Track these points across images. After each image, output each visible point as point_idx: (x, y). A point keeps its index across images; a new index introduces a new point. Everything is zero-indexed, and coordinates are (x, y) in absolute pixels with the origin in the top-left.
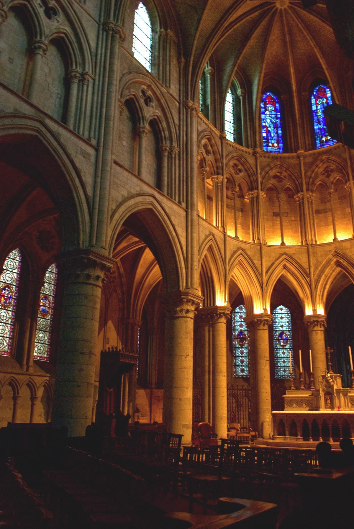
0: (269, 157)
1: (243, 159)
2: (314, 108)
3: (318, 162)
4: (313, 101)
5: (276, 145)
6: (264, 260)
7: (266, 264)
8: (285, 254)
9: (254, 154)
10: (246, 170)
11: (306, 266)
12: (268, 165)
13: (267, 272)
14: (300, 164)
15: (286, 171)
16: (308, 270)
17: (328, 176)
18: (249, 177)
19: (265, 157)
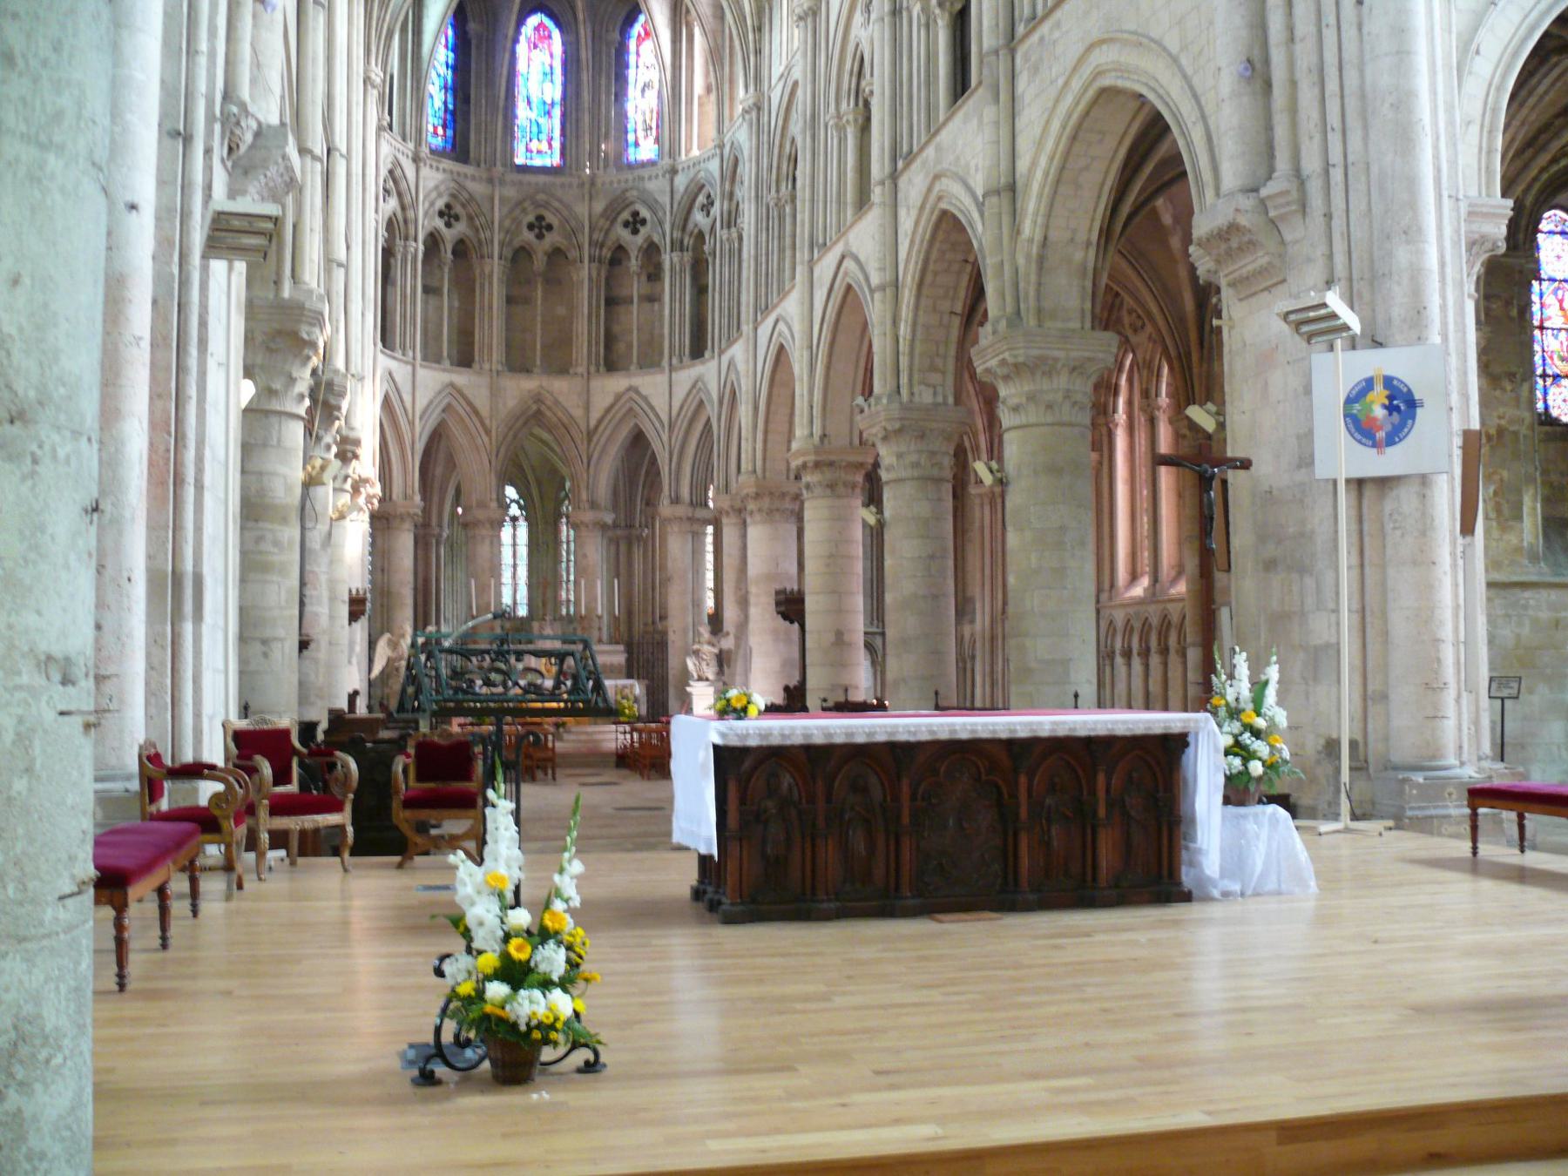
0: (438, 169)
1: (399, 170)
2: (521, 66)
3: (526, 204)
4: (522, 49)
5: (440, 131)
6: (418, 394)
7: (421, 404)
8: (452, 385)
9: (416, 159)
10: (400, 195)
11: (484, 412)
12: (436, 187)
13: (421, 418)
14: (492, 199)
15: (463, 206)
16: (487, 422)
17: (540, 237)
18: (403, 208)
19: (431, 166)
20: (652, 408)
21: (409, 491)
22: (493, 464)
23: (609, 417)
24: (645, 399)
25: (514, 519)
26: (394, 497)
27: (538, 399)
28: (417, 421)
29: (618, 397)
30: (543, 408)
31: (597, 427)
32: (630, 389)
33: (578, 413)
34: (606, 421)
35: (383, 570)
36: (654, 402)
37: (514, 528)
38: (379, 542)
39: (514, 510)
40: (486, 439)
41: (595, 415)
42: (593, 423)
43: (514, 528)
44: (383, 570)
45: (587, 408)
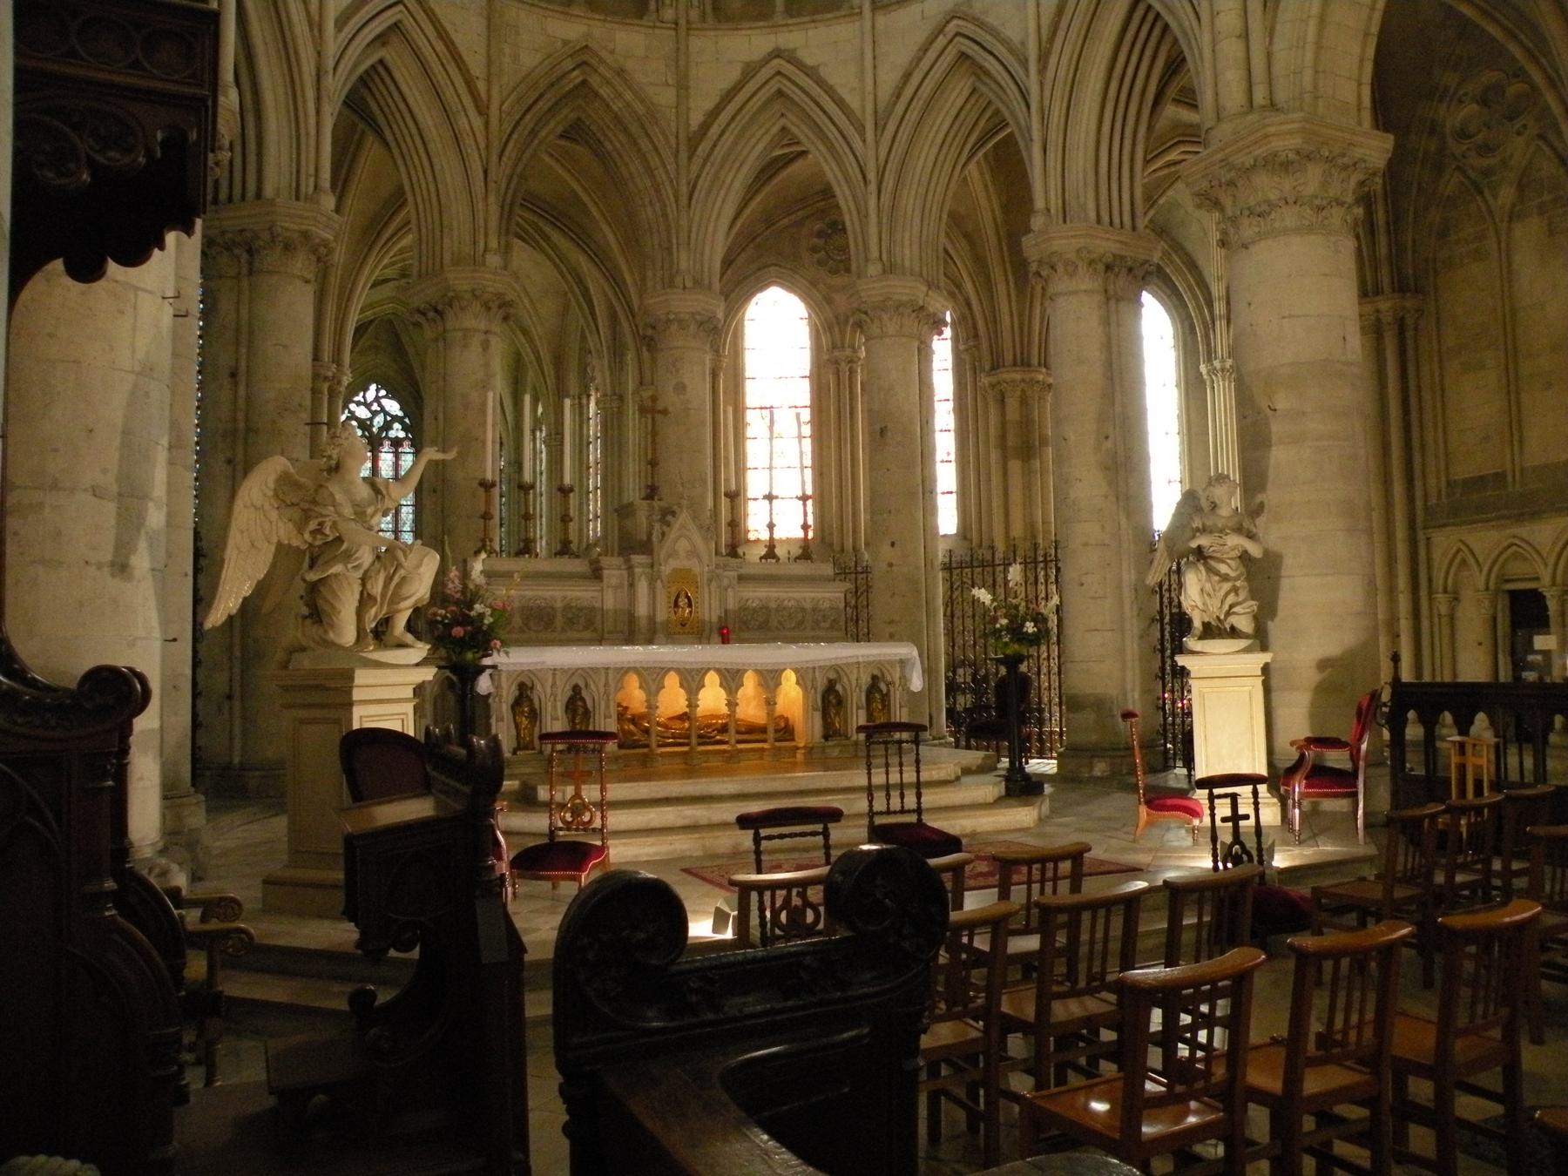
11: (476, 65)
16: (481, 86)
20: (830, 91)
21: (307, 186)
22: (492, 175)
23: (731, 109)
24: (812, 72)
25: (397, 443)
26: (269, 191)
27: (584, 56)
28: (330, 26)
29: (750, 71)
30: (594, 81)
31: (705, 127)
32: (777, 54)
33: (665, 97)
34: (724, 118)
35: (233, 375)
36: (833, 79)
37: (397, 455)
38: (225, 306)
39: (397, 431)
40: (478, 122)
41: (699, 106)
42: (696, 119)
43: (397, 455)
44: (233, 375)
45: (682, 86)
